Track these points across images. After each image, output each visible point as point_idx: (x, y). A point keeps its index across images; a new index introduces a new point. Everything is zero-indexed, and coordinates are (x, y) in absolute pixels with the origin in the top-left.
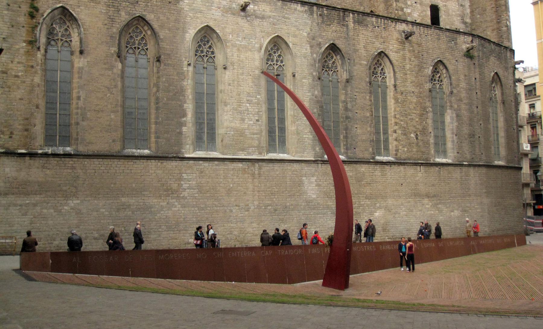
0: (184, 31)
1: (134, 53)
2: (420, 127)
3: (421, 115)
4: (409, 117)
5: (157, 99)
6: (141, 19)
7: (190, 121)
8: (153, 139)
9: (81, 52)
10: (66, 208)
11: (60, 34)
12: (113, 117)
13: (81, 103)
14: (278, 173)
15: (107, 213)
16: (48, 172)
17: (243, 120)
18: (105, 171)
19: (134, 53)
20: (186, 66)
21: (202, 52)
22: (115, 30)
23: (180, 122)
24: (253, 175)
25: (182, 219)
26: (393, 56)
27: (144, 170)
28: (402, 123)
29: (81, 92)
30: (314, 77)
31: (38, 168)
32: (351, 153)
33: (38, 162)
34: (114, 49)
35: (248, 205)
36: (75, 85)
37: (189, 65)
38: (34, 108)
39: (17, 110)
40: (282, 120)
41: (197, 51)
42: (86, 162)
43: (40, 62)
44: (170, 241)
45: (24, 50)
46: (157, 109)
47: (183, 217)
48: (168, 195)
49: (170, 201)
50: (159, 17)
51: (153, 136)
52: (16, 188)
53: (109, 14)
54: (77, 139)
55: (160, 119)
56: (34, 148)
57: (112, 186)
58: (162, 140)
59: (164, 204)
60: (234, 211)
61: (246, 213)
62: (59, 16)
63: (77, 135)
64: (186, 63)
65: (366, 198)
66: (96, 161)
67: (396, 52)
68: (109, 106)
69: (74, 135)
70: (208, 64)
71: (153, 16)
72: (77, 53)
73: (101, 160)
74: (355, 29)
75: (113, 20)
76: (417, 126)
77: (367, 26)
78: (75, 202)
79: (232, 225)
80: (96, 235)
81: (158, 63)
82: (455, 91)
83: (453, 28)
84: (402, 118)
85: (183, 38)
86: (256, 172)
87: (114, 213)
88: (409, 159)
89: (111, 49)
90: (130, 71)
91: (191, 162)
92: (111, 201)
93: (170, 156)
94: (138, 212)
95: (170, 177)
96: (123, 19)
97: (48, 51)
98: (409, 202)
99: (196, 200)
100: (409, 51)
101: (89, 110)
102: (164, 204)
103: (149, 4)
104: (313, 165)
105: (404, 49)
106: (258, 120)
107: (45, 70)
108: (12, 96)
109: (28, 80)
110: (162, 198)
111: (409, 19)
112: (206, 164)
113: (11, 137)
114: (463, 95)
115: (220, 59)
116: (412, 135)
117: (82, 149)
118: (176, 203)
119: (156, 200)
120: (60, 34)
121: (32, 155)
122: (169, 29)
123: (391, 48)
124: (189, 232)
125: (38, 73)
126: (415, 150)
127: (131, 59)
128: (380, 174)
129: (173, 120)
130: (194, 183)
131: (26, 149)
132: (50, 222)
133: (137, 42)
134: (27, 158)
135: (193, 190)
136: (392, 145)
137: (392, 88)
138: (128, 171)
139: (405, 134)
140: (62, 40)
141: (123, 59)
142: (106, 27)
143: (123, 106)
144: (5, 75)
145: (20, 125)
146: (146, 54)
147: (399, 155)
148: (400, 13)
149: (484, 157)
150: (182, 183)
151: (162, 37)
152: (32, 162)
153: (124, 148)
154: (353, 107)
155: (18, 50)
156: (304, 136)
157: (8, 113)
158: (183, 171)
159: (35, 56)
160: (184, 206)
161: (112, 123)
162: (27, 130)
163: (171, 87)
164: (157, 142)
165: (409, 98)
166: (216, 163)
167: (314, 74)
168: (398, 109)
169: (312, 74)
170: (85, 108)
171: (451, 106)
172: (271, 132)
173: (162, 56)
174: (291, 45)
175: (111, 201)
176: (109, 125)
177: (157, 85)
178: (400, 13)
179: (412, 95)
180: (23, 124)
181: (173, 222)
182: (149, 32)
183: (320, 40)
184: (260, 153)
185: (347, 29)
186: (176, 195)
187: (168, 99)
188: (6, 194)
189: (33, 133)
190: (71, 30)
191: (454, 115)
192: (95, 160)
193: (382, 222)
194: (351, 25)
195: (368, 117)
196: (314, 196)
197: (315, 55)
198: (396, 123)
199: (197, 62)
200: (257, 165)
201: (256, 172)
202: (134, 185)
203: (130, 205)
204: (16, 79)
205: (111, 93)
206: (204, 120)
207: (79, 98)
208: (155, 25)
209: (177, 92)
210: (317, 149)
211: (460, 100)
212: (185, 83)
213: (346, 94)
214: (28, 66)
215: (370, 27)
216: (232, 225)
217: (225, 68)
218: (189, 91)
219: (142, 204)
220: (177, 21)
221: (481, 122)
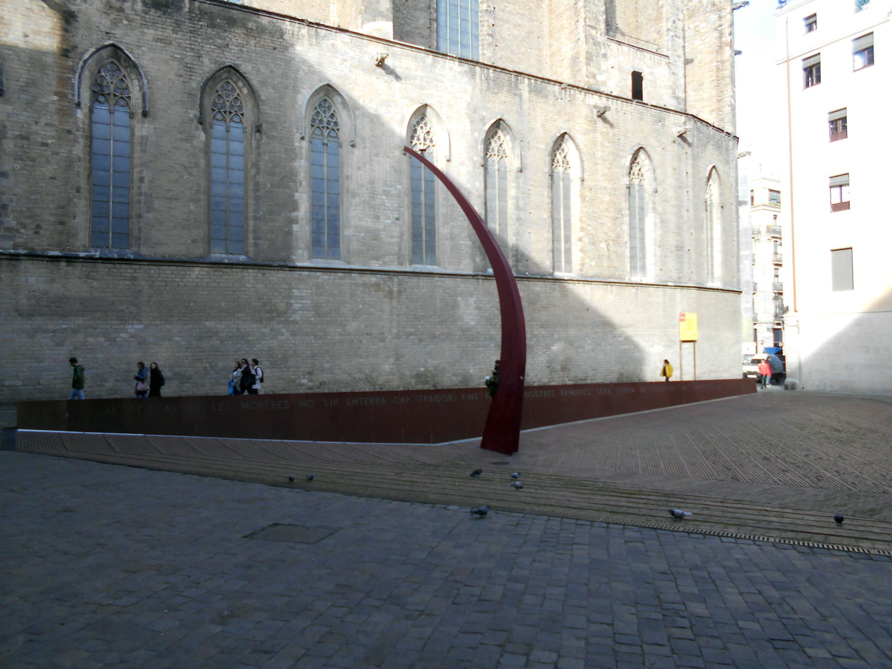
0: (296, 90)
1: (224, 120)
2: (613, 235)
3: (615, 219)
4: (600, 221)
5: (257, 184)
6: (233, 69)
8: (251, 241)
9: (145, 114)
10: (123, 335)
11: (112, 87)
12: (192, 207)
13: (145, 187)
14: (424, 291)
15: (184, 343)
16: (95, 284)
17: (377, 217)
18: (181, 284)
19: (224, 120)
21: (321, 121)
22: (194, 85)
24: (391, 292)
25: (291, 352)
26: (579, 138)
28: (590, 228)
29: (145, 172)
30: (474, 163)
31: (79, 278)
32: (523, 266)
33: (78, 270)
34: (194, 113)
35: (383, 334)
36: (136, 161)
37: (302, 138)
38: (74, 191)
39: (47, 195)
40: (431, 220)
41: (313, 120)
42: (153, 270)
43: (81, 125)
45: (56, 106)
46: (257, 199)
48: (272, 319)
49: (275, 326)
50: (259, 70)
51: (251, 236)
52: (46, 307)
53: (186, 61)
54: (139, 238)
57: (192, 304)
59: (267, 331)
60: (364, 341)
61: (381, 344)
62: (110, 60)
63: (139, 232)
64: (298, 136)
65: (542, 326)
66: (167, 270)
67: (584, 134)
69: (136, 233)
70: (330, 138)
71: (250, 68)
72: (139, 116)
73: (175, 268)
74: (530, 101)
75: (189, 69)
76: (610, 234)
77: (547, 97)
78: (136, 327)
79: (361, 360)
81: (257, 134)
82: (660, 189)
83: (661, 105)
84: (589, 222)
85: (295, 101)
86: (395, 289)
87: (194, 342)
88: (598, 277)
89: (189, 111)
90: (218, 145)
92: (191, 326)
95: (275, 294)
96: (207, 69)
97: (95, 110)
98: (597, 333)
100: (602, 133)
102: (267, 331)
103: (245, 49)
104: (472, 281)
105: (595, 131)
106: (397, 219)
107: (90, 138)
108: (38, 173)
109: (63, 152)
111: (602, 89)
112: (325, 277)
114: (671, 194)
115: (345, 133)
116: (603, 245)
117: (145, 251)
118: (284, 330)
119: (255, 326)
120: (112, 87)
121: (71, 259)
122: (274, 88)
123: (578, 128)
124: (302, 369)
125: (78, 142)
126: (605, 265)
127: (219, 129)
128: (559, 295)
130: (309, 302)
131: (61, 251)
132: (100, 356)
133: (228, 104)
134: (63, 264)
136: (576, 256)
137: (579, 182)
138: (214, 285)
139: (593, 244)
140: (115, 95)
141: (208, 126)
142: (182, 79)
143: (209, 194)
144: (25, 142)
145: (51, 215)
146: (241, 122)
147: (585, 270)
148: (592, 81)
149: (694, 277)
150: (292, 301)
151: (263, 98)
152: (70, 269)
154: (525, 205)
155: (46, 105)
156: (461, 242)
159: (72, 115)
160: (293, 334)
161: (192, 216)
162: (61, 223)
163: (278, 170)
164: (256, 245)
165: (600, 195)
166: (340, 275)
167: (476, 159)
168: (585, 210)
169: (472, 159)
170: (151, 195)
171: (654, 209)
172: (416, 236)
174: (443, 117)
175: (191, 326)
176: (187, 220)
177: (256, 165)
178: (592, 81)
179: (604, 191)
180: (57, 215)
182: (245, 91)
183: (484, 113)
184: (401, 264)
185: (521, 100)
187: (272, 186)
188: (30, 315)
190: (128, 82)
191: (658, 221)
192: (165, 268)
193: (561, 358)
194: (526, 94)
195: (545, 220)
196: (473, 323)
197: (476, 134)
198: (582, 229)
199: (314, 136)
200: (396, 279)
201: (395, 289)
202: (223, 304)
204: (43, 148)
205: (190, 174)
206: (323, 215)
207: (141, 180)
208: (255, 82)
210: (478, 259)
211: (666, 201)
212: (296, 164)
213: (518, 187)
214: (63, 130)
215: (551, 99)
216: (361, 360)
217: (353, 146)
218: (302, 175)
219: (235, 330)
220: (285, 75)
221: (692, 231)
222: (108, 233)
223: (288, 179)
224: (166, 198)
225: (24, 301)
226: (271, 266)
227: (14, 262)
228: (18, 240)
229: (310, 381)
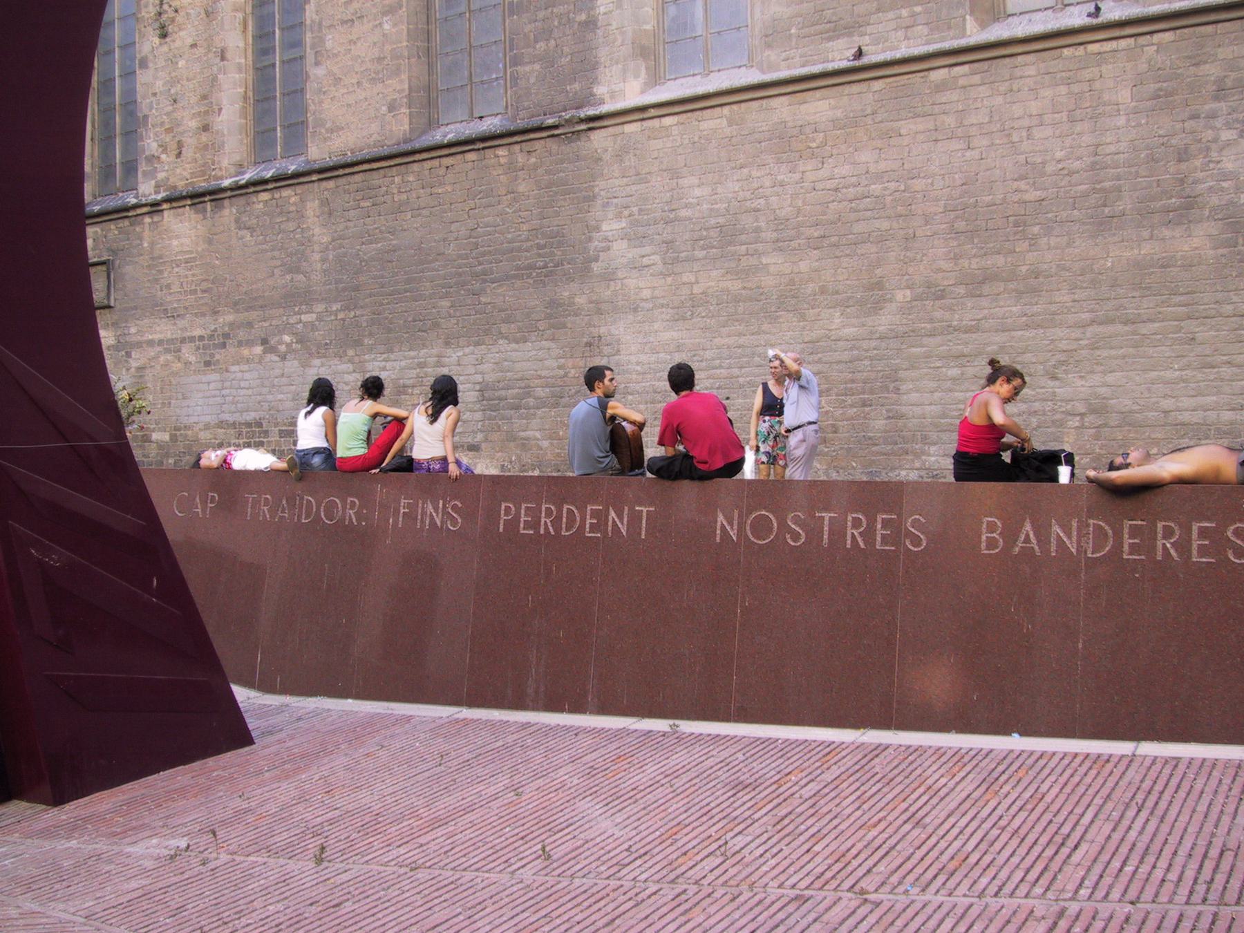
35: (879, 285)
56: (220, 174)
58: (528, 68)
91: (628, 128)
101: (332, 26)
117: (317, 152)
153: (432, 124)
161: (388, 47)
162: (205, 128)
170: (320, 24)
176: (380, 59)
189: (218, 132)
222: (275, 130)
224: (344, 22)
227: (156, 218)
228: (161, 176)
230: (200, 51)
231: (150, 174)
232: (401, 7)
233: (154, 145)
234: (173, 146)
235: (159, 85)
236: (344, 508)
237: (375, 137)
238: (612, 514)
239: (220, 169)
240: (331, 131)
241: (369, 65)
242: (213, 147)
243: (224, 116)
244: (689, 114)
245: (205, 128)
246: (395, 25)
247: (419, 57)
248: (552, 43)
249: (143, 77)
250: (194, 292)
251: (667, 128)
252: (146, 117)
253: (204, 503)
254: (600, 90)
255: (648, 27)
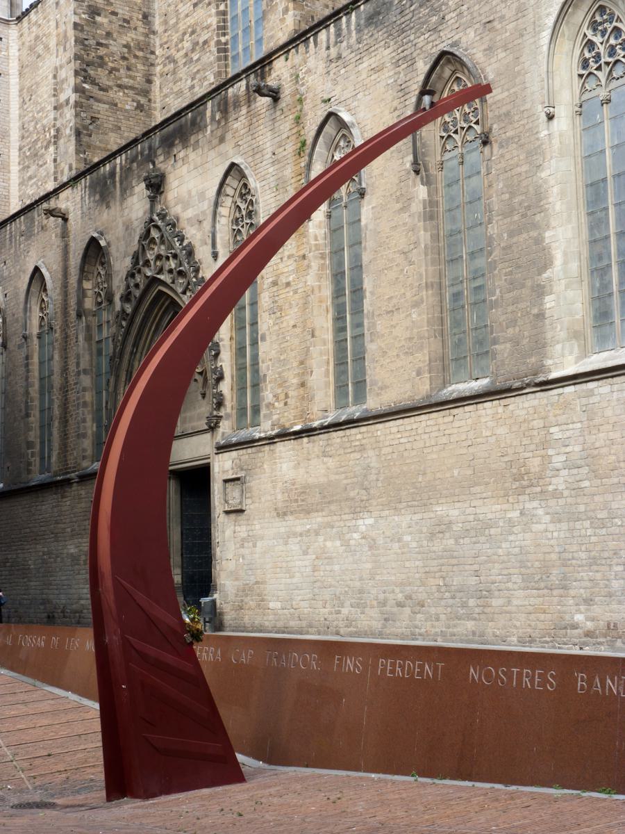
7: (561, 275)
20: (545, 124)
23: (539, 285)
27: (472, 432)
37: (550, 117)
42: (380, 429)
44: (532, 617)
47: (557, 549)
48: (521, 491)
49: (528, 505)
53: (399, 82)
55: (498, 291)
56: (312, 417)
58: (502, 347)
66: (393, 426)
68: (409, 294)
80: (400, 597)
87: (425, 543)
93: (517, 384)
94: (467, 540)
99: (586, 500)
102: (514, 515)
110: (511, 500)
113: (286, 404)
117: (373, 403)
118: (540, 512)
121: (308, 432)
129: (523, 286)
132: (336, 567)
135: (575, 471)
138: (444, 440)
141: (433, 171)
150: (551, 452)
152: (311, 445)
153: (445, 384)
157: (282, 358)
158: (552, 419)
170: (373, 312)
173: (495, 126)
176: (410, 339)
181: (537, 564)
186: (538, 489)
187: (511, 234)
202: (456, 472)
203: (450, 523)
209: (529, 208)
219: (471, 518)
222: (348, 385)
223: (529, 211)
224: (388, 312)
225: (279, 497)
226: (509, 390)
227: (272, 447)
229: (587, 619)
230: (298, 330)
231: (268, 416)
232: (422, 302)
233: (271, 396)
234: (282, 396)
235: (273, 354)
236: (310, 660)
237: (409, 393)
238: (427, 667)
239: (312, 414)
240: (381, 388)
241: (403, 343)
242: (307, 398)
243: (314, 376)
244: (605, 380)
245: (303, 385)
246: (419, 315)
247: (436, 337)
248: (517, 329)
249: (263, 347)
250: (296, 501)
251: (592, 390)
252: (265, 376)
253: (246, 655)
254: (549, 362)
255: (577, 317)
